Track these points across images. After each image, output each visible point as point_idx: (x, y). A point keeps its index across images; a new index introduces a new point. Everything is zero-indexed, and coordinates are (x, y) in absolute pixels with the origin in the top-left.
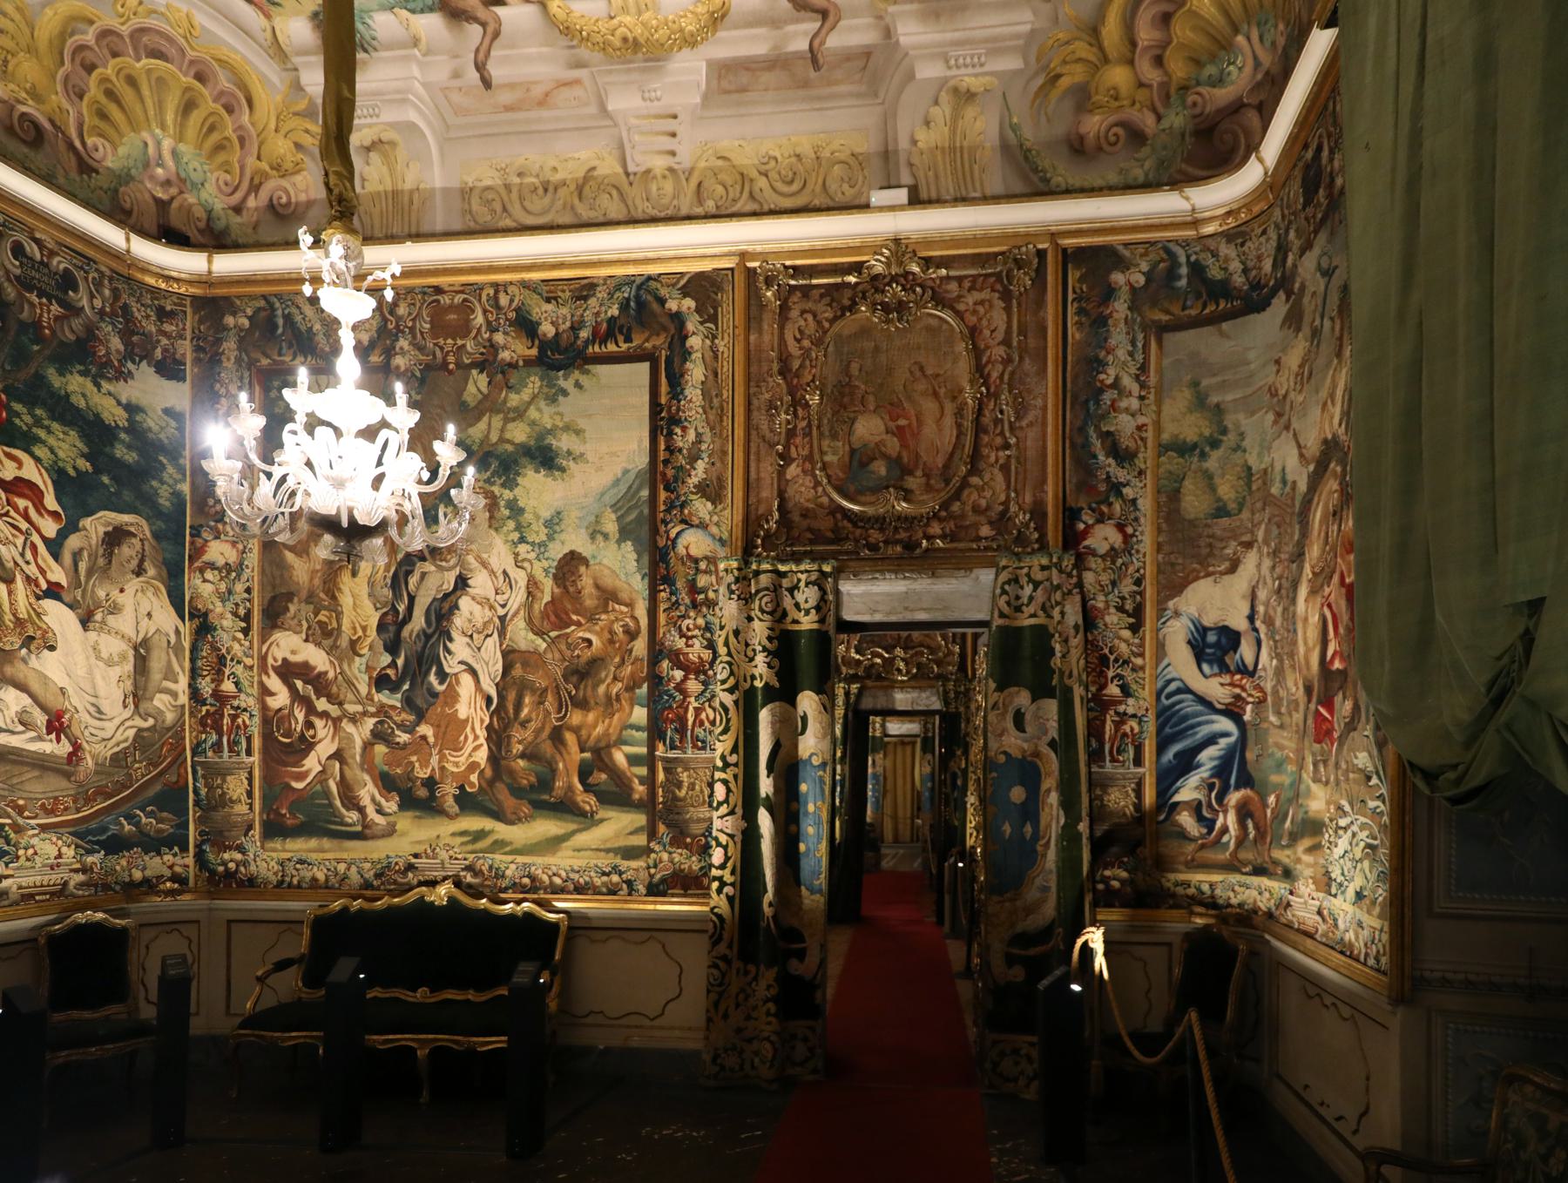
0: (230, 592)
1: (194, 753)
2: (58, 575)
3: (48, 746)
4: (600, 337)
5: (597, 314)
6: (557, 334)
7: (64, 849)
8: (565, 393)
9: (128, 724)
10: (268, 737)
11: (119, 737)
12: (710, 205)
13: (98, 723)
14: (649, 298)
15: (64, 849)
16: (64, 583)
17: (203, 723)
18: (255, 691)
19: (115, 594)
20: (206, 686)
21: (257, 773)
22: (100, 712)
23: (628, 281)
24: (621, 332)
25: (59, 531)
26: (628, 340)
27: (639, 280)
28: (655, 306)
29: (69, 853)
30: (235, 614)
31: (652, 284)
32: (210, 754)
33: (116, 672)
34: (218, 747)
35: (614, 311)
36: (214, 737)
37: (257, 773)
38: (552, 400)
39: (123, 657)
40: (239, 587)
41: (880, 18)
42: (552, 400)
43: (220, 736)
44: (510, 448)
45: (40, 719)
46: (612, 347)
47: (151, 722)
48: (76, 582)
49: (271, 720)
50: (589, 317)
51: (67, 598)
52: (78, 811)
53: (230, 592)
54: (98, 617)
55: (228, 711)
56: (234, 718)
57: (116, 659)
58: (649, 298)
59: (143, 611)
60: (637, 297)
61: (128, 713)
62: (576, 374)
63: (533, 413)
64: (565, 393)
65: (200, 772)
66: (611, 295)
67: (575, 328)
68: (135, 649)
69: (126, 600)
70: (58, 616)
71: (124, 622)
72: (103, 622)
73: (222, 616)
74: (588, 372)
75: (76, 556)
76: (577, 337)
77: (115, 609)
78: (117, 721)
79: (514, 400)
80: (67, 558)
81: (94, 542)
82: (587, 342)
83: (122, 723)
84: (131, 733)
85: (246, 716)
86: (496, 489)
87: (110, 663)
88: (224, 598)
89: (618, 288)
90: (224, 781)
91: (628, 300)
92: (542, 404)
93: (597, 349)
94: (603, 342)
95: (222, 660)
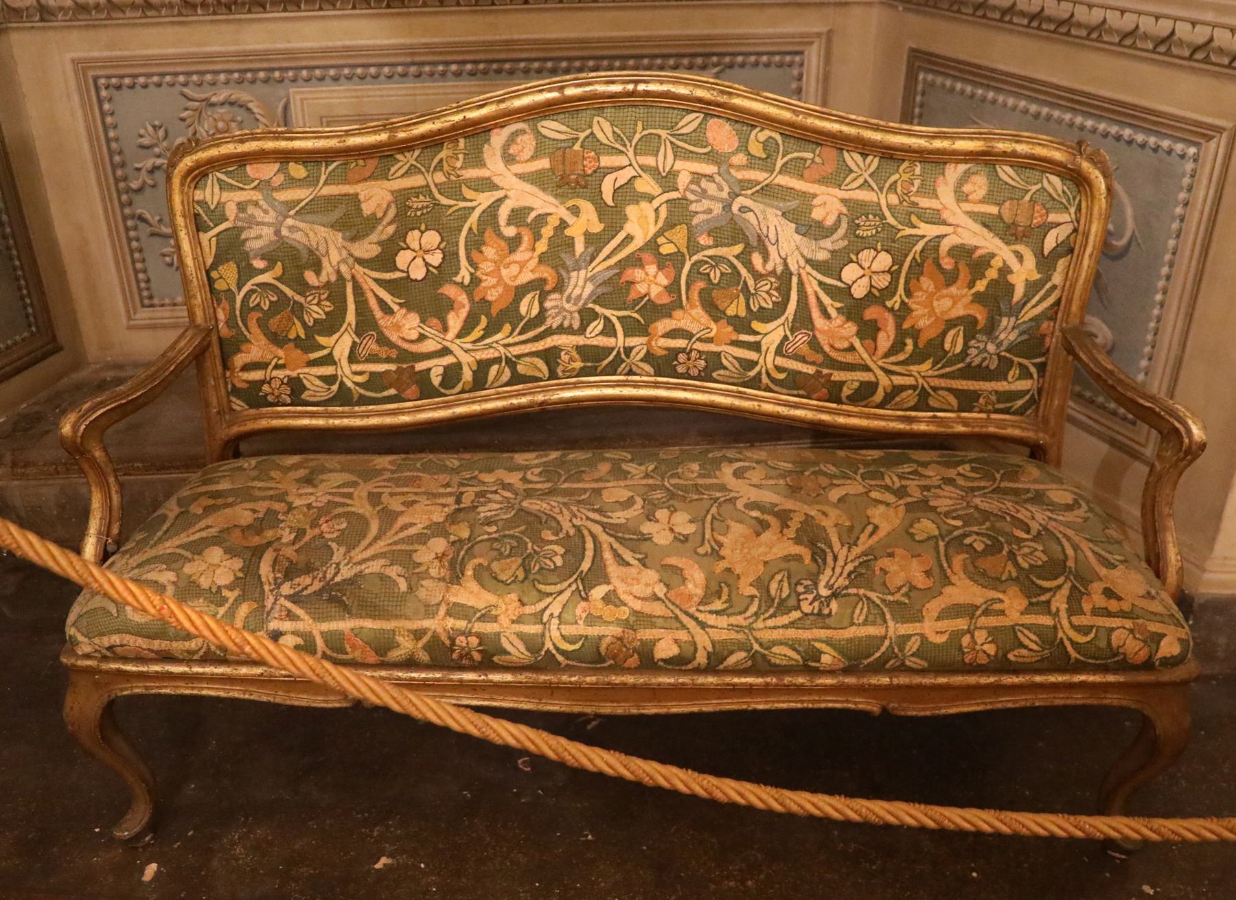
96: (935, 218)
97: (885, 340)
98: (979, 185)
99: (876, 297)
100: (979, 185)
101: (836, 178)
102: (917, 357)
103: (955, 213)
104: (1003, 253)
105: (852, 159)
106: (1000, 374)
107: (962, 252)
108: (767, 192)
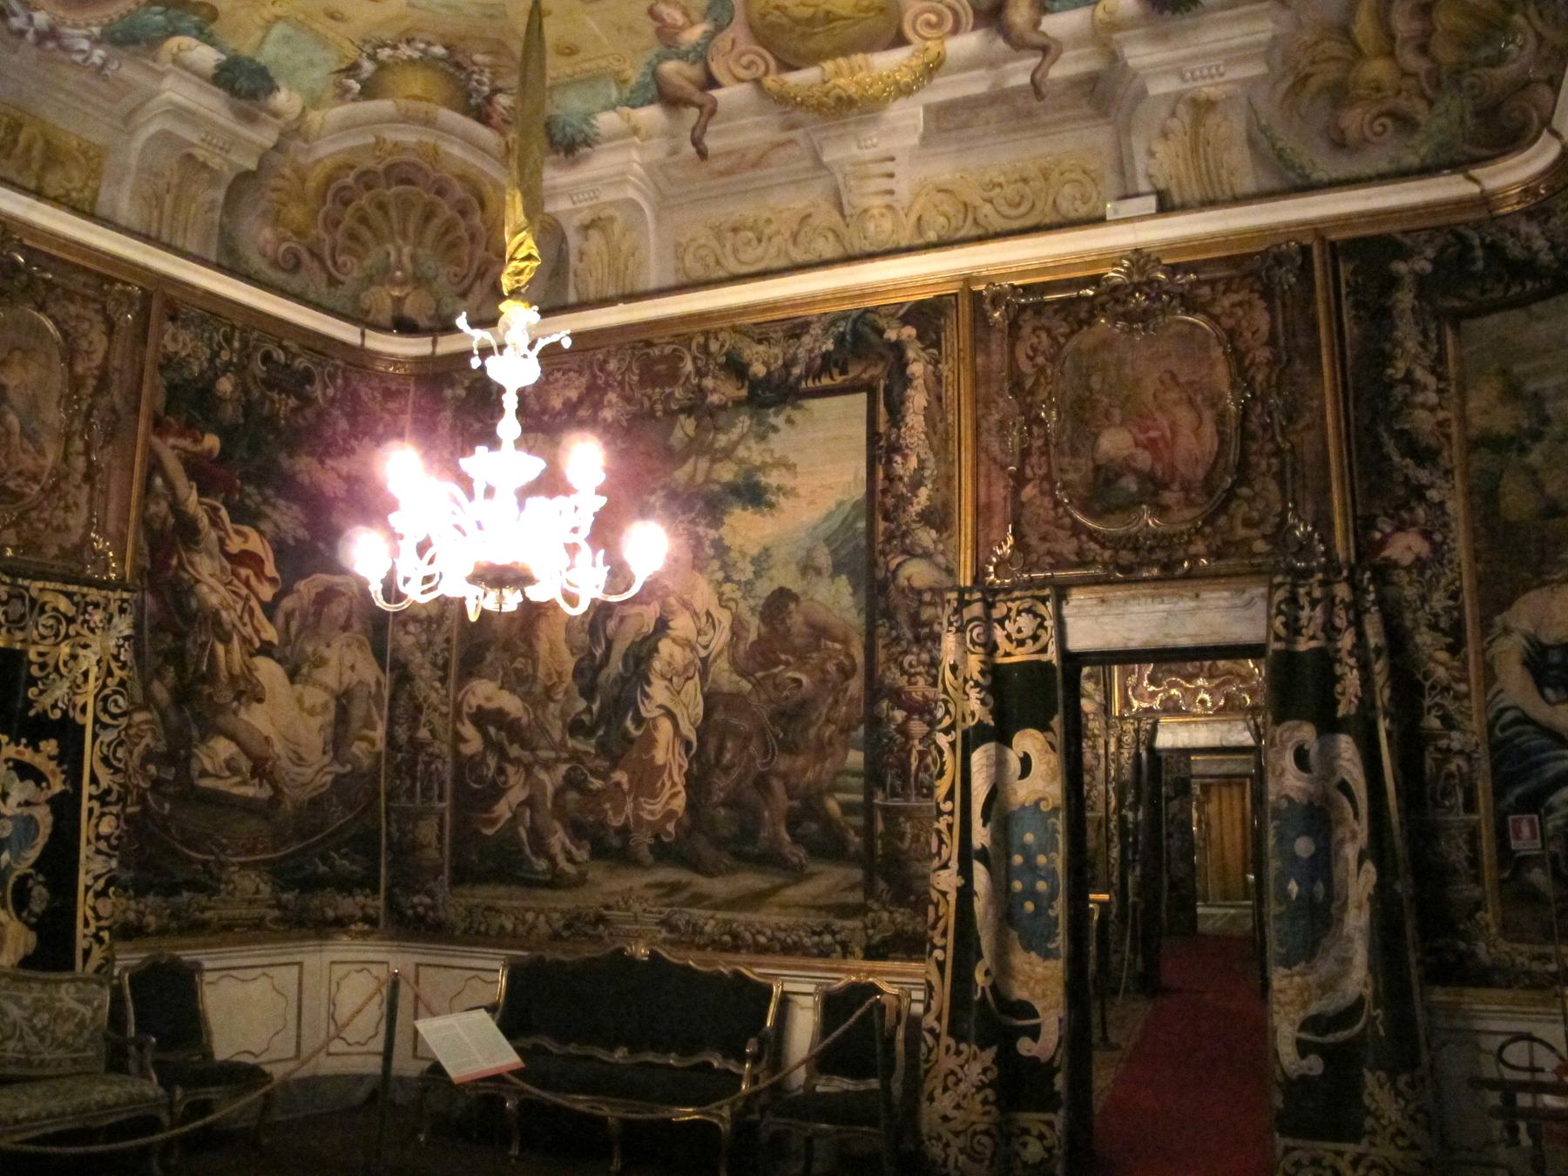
0: (430, 643)
1: (389, 797)
2: (271, 634)
3: (250, 791)
4: (812, 372)
5: (811, 351)
6: (769, 373)
7: (262, 886)
8: (775, 429)
9: (328, 769)
10: (458, 779)
11: (318, 781)
12: (932, 236)
13: (297, 769)
14: (867, 330)
15: (262, 886)
16: (276, 641)
17: (397, 769)
18: (449, 736)
19: (323, 650)
20: (402, 734)
21: (448, 818)
22: (301, 758)
23: (844, 316)
24: (836, 365)
25: (275, 596)
26: (843, 372)
27: (855, 315)
28: (873, 338)
29: (266, 890)
30: (434, 664)
31: (870, 316)
32: (403, 799)
33: (316, 722)
34: (411, 793)
35: (829, 345)
36: (408, 782)
37: (448, 818)
38: (762, 438)
39: (325, 706)
40: (439, 639)
41: (1105, 45)
42: (762, 438)
43: (414, 779)
44: (716, 488)
45: (245, 765)
46: (826, 381)
47: (349, 767)
48: (286, 639)
49: (465, 766)
50: (802, 354)
51: (277, 655)
52: (275, 850)
53: (430, 643)
54: (305, 670)
55: (422, 757)
56: (428, 764)
57: (318, 709)
58: (867, 330)
59: (347, 663)
60: (854, 332)
61: (326, 759)
62: (788, 410)
63: (741, 452)
64: (775, 429)
65: (393, 816)
66: (826, 330)
67: (788, 365)
68: (338, 698)
69: (332, 655)
70: (268, 671)
71: (329, 676)
72: (309, 675)
73: (421, 666)
74: (800, 407)
75: (289, 616)
76: (789, 374)
77: (321, 662)
78: (316, 767)
79: (722, 440)
80: (280, 619)
81: (306, 602)
82: (799, 379)
83: (321, 769)
84: (329, 778)
85: (438, 764)
86: (701, 530)
87: (312, 712)
88: (424, 648)
89: (833, 323)
90: (416, 826)
91: (843, 334)
92: (752, 443)
93: (810, 383)
94: (817, 376)
95: (419, 709)
96: (60, 1000)
97: (48, 1041)
98: (72, 989)
99: (45, 1028)
100: (72, 989)
101: (30, 990)
102: (58, 1047)
103: (67, 999)
104: (82, 1008)
105: (33, 985)
106: (84, 1050)
107: (70, 1010)
108: (8, 997)
